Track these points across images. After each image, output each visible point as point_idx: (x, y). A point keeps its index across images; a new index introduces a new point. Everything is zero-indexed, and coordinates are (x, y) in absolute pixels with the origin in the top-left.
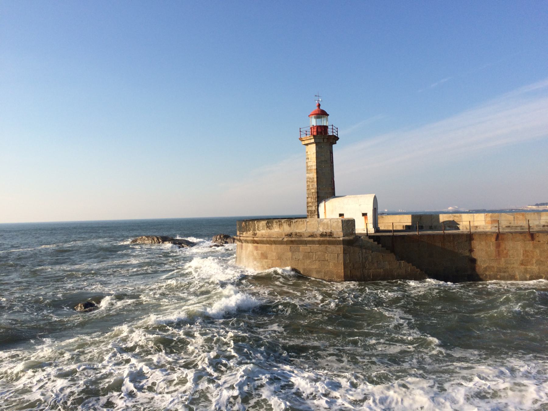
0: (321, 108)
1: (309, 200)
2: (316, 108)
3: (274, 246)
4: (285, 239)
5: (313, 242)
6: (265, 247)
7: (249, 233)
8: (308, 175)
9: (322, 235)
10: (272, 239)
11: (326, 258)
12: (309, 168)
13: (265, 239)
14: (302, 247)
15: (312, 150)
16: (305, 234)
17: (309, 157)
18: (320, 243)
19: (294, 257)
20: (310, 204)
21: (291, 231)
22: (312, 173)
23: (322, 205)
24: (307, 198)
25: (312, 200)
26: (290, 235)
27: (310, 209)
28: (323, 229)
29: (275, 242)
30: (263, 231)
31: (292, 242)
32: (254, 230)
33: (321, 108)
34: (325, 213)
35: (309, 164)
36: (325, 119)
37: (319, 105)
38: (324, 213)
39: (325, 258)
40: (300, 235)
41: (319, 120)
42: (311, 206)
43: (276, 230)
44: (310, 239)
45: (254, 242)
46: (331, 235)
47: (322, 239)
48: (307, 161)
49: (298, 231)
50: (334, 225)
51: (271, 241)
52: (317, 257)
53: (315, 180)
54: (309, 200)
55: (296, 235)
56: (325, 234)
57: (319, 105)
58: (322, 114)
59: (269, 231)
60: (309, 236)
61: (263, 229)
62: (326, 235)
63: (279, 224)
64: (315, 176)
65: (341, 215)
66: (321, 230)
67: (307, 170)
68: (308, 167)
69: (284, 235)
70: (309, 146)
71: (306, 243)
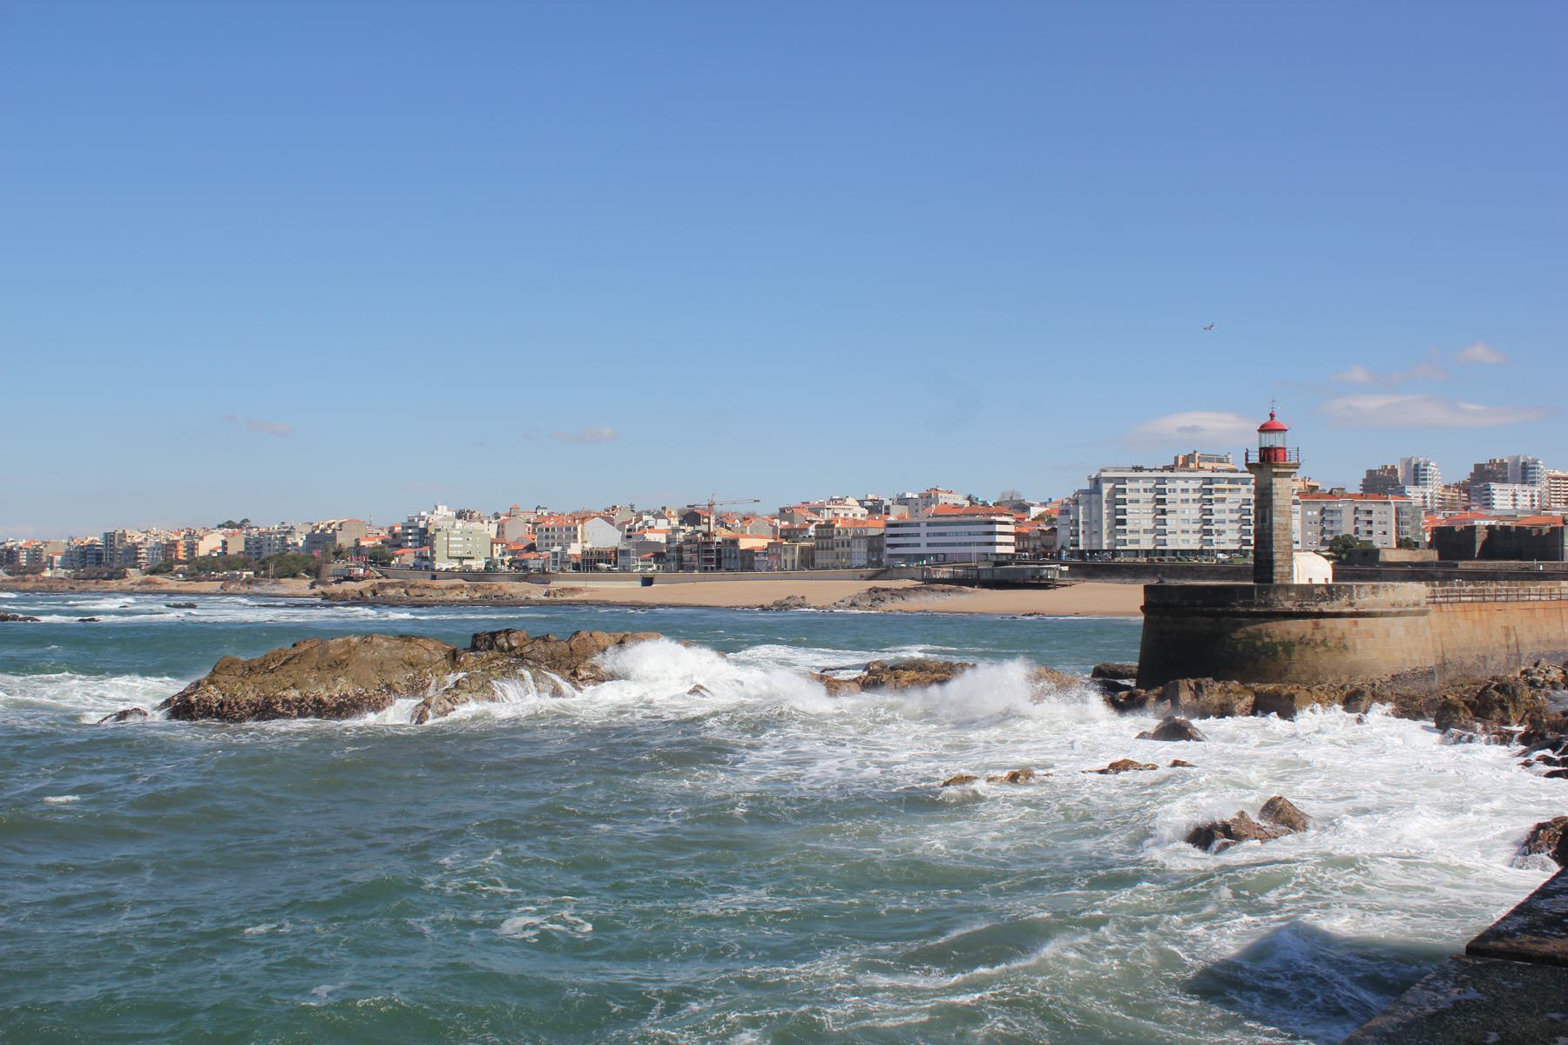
3: (1380, 619)
45: (1351, 615)
57: (1272, 416)
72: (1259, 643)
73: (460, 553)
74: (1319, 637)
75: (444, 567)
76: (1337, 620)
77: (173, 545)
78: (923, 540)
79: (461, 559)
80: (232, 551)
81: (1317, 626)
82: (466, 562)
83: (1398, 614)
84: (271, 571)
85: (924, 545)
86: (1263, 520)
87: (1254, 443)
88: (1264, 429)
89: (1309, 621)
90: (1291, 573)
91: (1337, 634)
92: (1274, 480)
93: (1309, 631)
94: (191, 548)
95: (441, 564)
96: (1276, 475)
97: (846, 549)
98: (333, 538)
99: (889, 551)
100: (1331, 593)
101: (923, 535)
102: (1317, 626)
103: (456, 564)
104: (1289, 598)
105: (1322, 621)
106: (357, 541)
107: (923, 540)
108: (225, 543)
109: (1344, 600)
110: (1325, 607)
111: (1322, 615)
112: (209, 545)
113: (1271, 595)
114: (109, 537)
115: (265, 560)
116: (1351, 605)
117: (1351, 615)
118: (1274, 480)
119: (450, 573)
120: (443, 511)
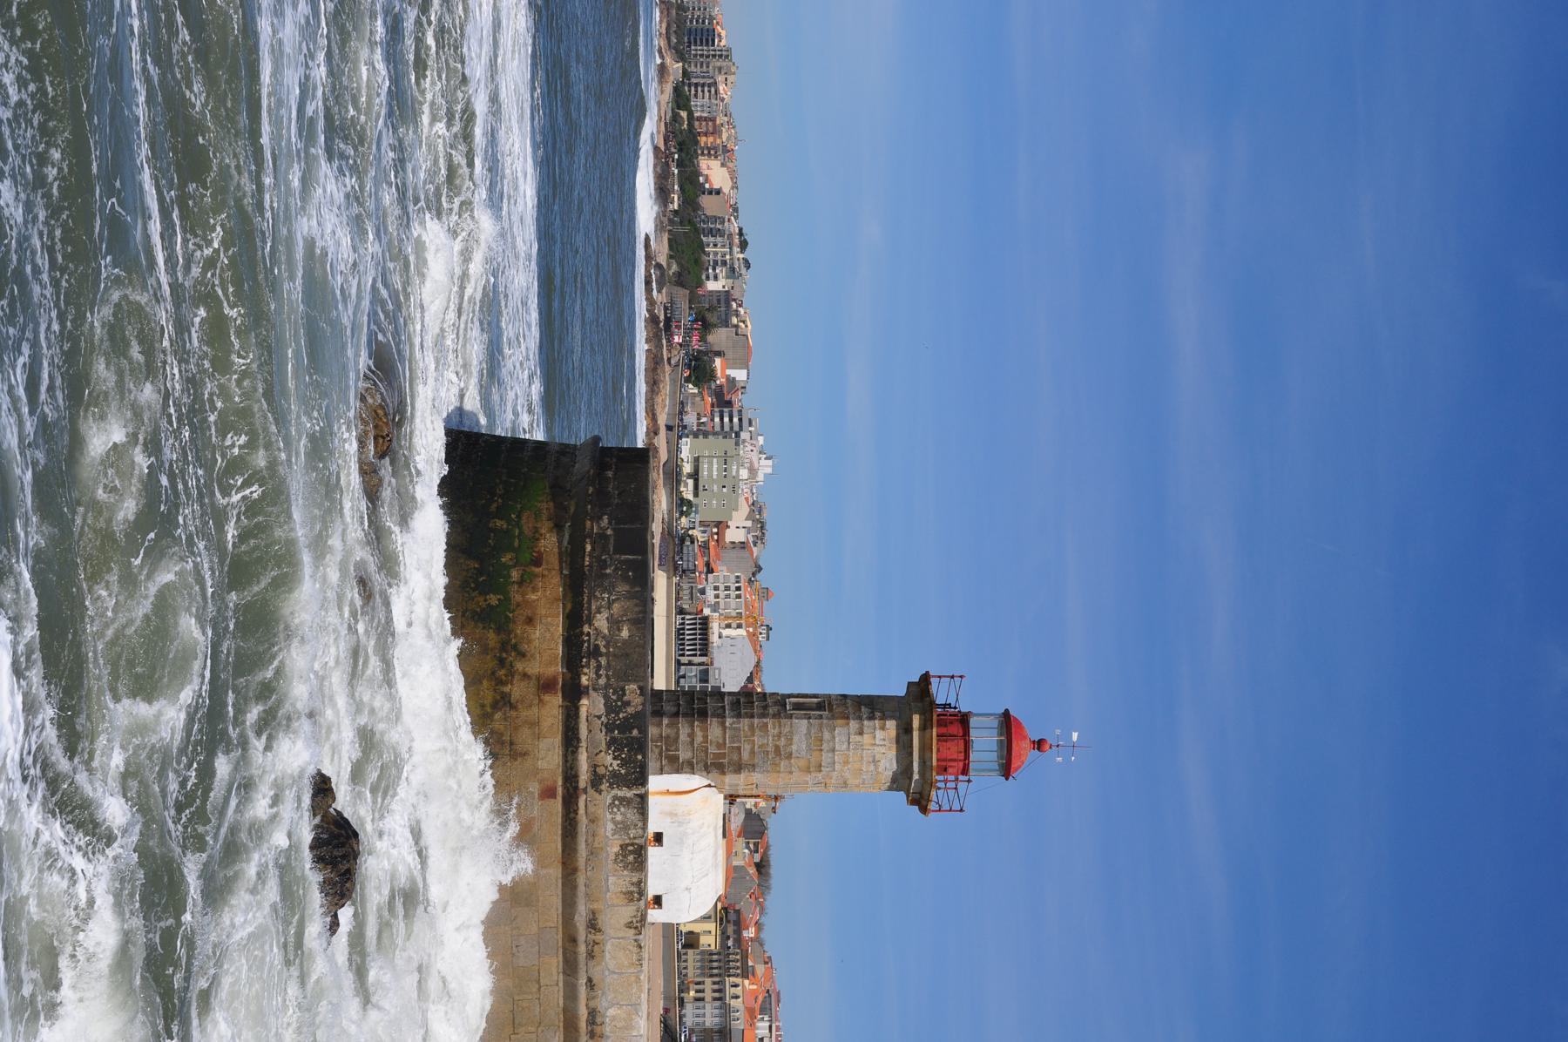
7: (602, 737)
9: (593, 1013)
10: (581, 879)
11: (522, 1030)
12: (827, 735)
14: (554, 963)
16: (598, 968)
17: (866, 738)
19: (522, 941)
20: (699, 738)
21: (610, 932)
22: (809, 749)
25: (712, 749)
26: (593, 925)
28: (614, 1018)
31: (570, 939)
32: (617, 780)
34: (668, 792)
37: (1039, 745)
38: (664, 788)
39: (520, 1025)
42: (692, 735)
43: (611, 879)
45: (570, 777)
47: (583, 1025)
49: (608, 947)
51: (575, 870)
52: (525, 1004)
55: (596, 943)
56: (599, 1020)
57: (1039, 745)
62: (594, 1023)
63: (632, 893)
65: (658, 838)
66: (611, 1012)
69: (595, 906)
71: (570, 967)
72: (506, 559)
73: (704, 473)
74: (517, 690)
75: (685, 453)
76: (557, 740)
77: (716, 132)
79: (695, 475)
80: (706, 201)
81: (546, 686)
82: (691, 482)
83: (570, 939)
84: (680, 229)
86: (798, 707)
87: (975, 697)
88: (1007, 723)
89: (558, 669)
91: (524, 736)
92: (891, 725)
93: (534, 668)
94: (712, 152)
95: (687, 449)
96: (905, 730)
97: (708, 995)
98: (726, 323)
100: (625, 726)
102: (546, 686)
103: (687, 468)
104: (615, 624)
105: (555, 701)
106: (719, 354)
108: (718, 192)
109: (609, 761)
110: (592, 705)
111: (573, 693)
112: (714, 172)
113: (622, 588)
114: (725, 55)
115: (690, 229)
116: (596, 781)
117: (570, 777)
118: (891, 725)
119: (674, 450)
120: (765, 467)
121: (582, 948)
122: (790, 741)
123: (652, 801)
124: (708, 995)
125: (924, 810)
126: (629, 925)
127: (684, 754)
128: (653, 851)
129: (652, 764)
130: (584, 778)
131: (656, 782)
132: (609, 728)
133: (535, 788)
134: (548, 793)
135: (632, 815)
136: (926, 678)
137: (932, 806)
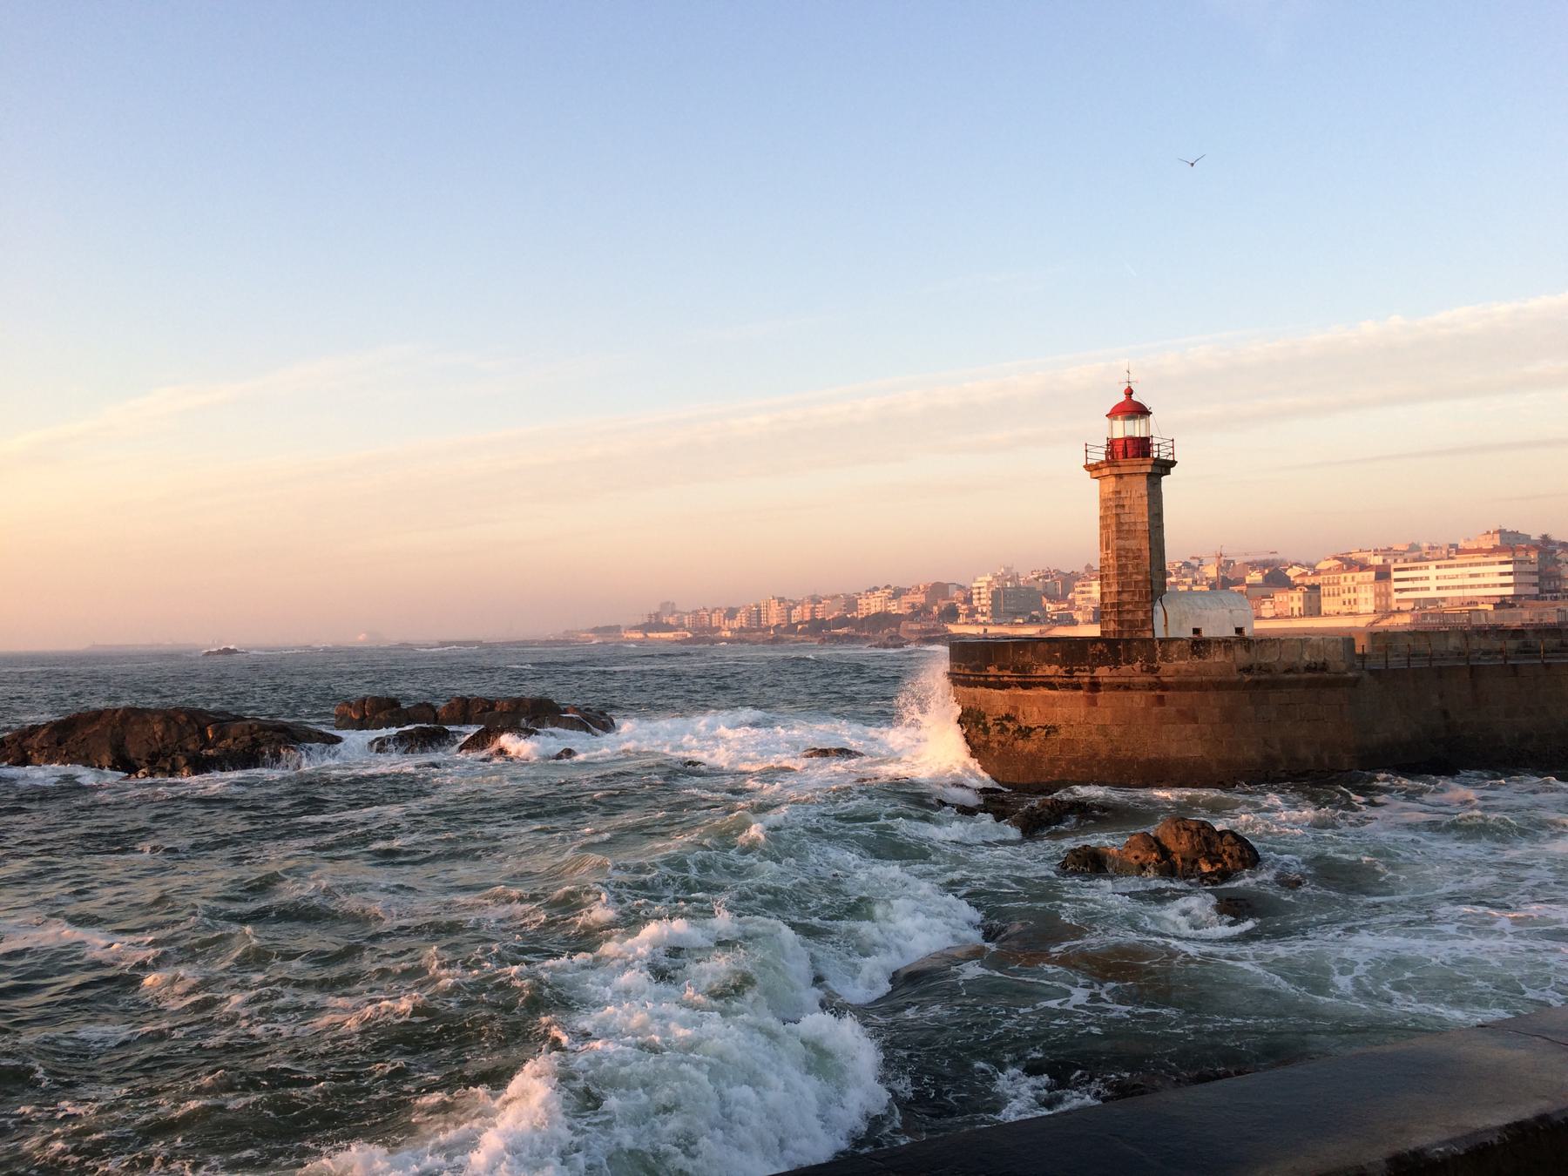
0: (1134, 398)
1: (1125, 597)
2: (1122, 398)
3: (1212, 696)
4: (1247, 678)
5: (1297, 683)
6: (1186, 699)
7: (1125, 668)
8: (1122, 542)
9: (1308, 669)
12: (1126, 527)
13: (1197, 679)
15: (1140, 486)
18: (1310, 684)
23: (1158, 608)
24: (1119, 593)
26: (1248, 670)
27: (1129, 617)
29: (1218, 686)
30: (1182, 664)
31: (1258, 683)
32: (1151, 659)
33: (1134, 398)
35: (1124, 519)
36: (1143, 421)
37: (1129, 392)
40: (1268, 669)
41: (1129, 423)
42: (1129, 611)
44: (1291, 676)
45: (1151, 687)
46: (1324, 667)
48: (1120, 511)
50: (1330, 647)
53: (1147, 553)
54: (1125, 597)
57: (1129, 392)
58: (1140, 411)
59: (1197, 661)
60: (1288, 671)
61: (1180, 658)
64: (1145, 545)
65: (1196, 631)
66: (1307, 658)
67: (1119, 531)
68: (1119, 524)
70: (1126, 478)
71: (1275, 685)
78: (1433, 584)
85: (1433, 588)
90: (1149, 620)
97: (1352, 596)
99: (1397, 596)
101: (1433, 578)
107: (1433, 584)
117: (1151, 687)
121: (1264, 677)
122: (1127, 550)
123: (1171, 635)
124: (1352, 596)
125: (1173, 463)
126: (1247, 649)
127: (1141, 615)
128: (1205, 634)
129: (1149, 635)
130: (1152, 679)
131: (1160, 633)
132: (1117, 663)
133: (1156, 710)
134: (1160, 701)
135: (1174, 648)
136: (1088, 467)
137: (1170, 458)
